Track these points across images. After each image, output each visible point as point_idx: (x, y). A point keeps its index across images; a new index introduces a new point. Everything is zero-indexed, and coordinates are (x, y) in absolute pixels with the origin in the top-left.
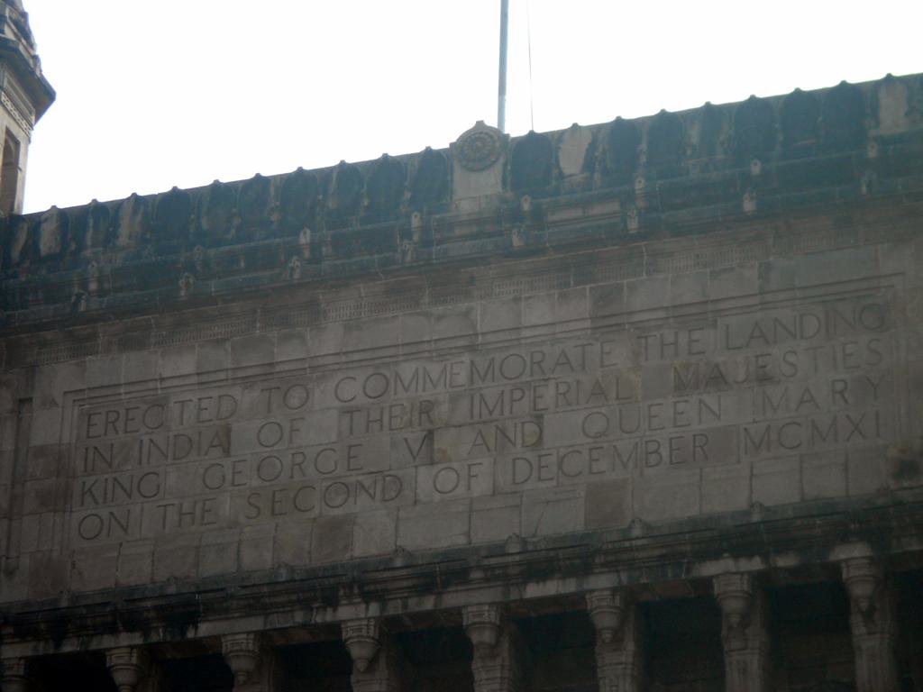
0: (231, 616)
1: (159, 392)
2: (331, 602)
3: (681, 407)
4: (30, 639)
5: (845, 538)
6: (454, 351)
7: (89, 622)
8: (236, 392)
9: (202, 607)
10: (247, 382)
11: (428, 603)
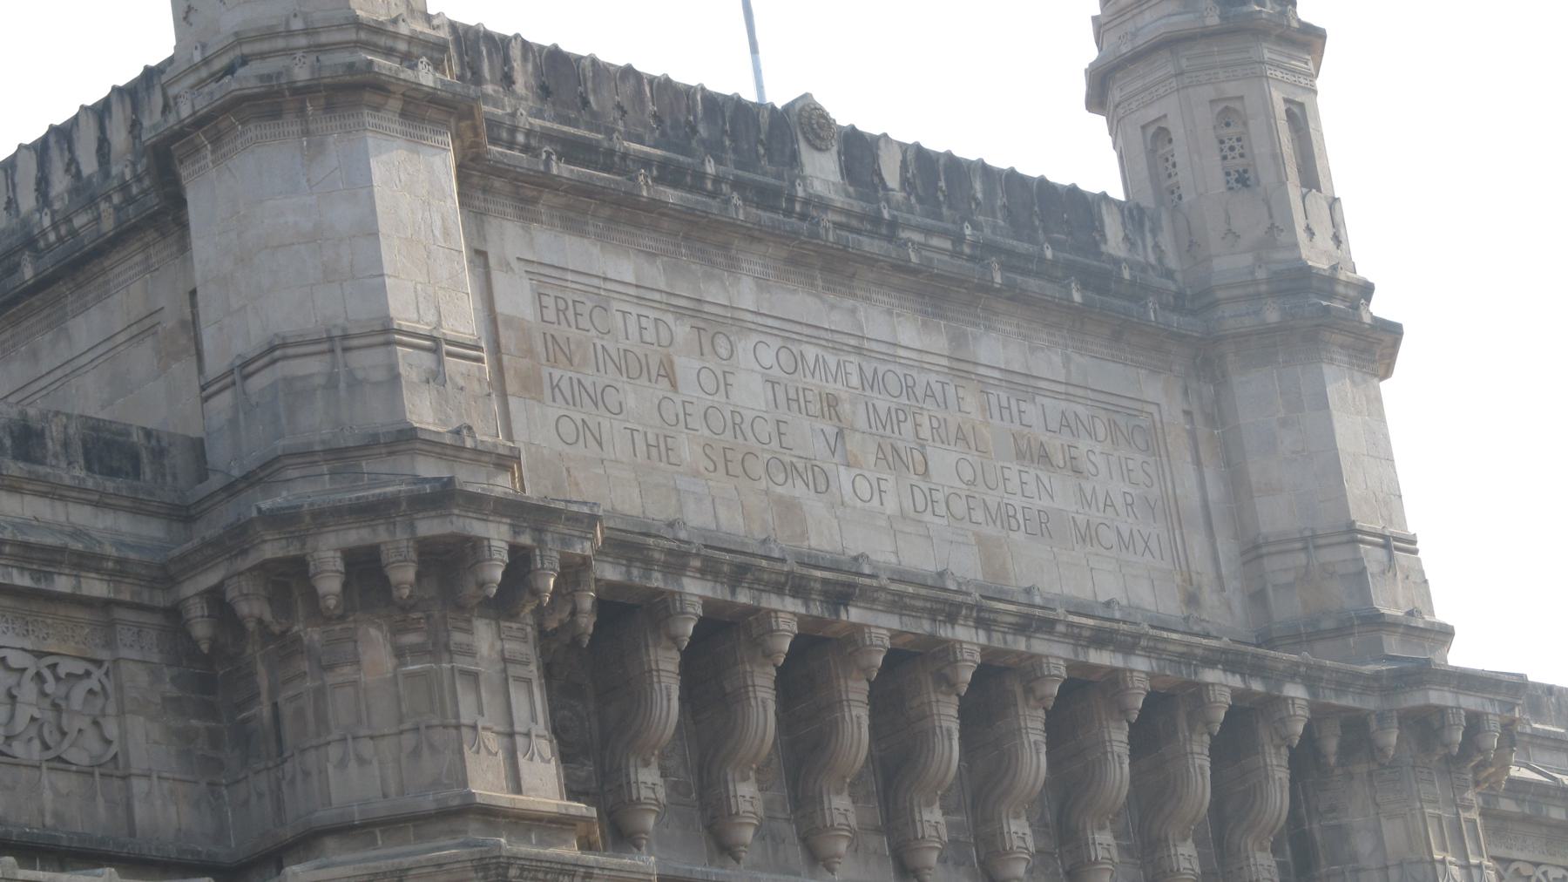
0: (875, 607)
1: (602, 293)
2: (952, 619)
3: (1025, 477)
4: (709, 577)
5: (1293, 674)
6: (845, 348)
7: (766, 576)
8: (669, 318)
9: (857, 591)
10: (680, 312)
11: (1021, 644)
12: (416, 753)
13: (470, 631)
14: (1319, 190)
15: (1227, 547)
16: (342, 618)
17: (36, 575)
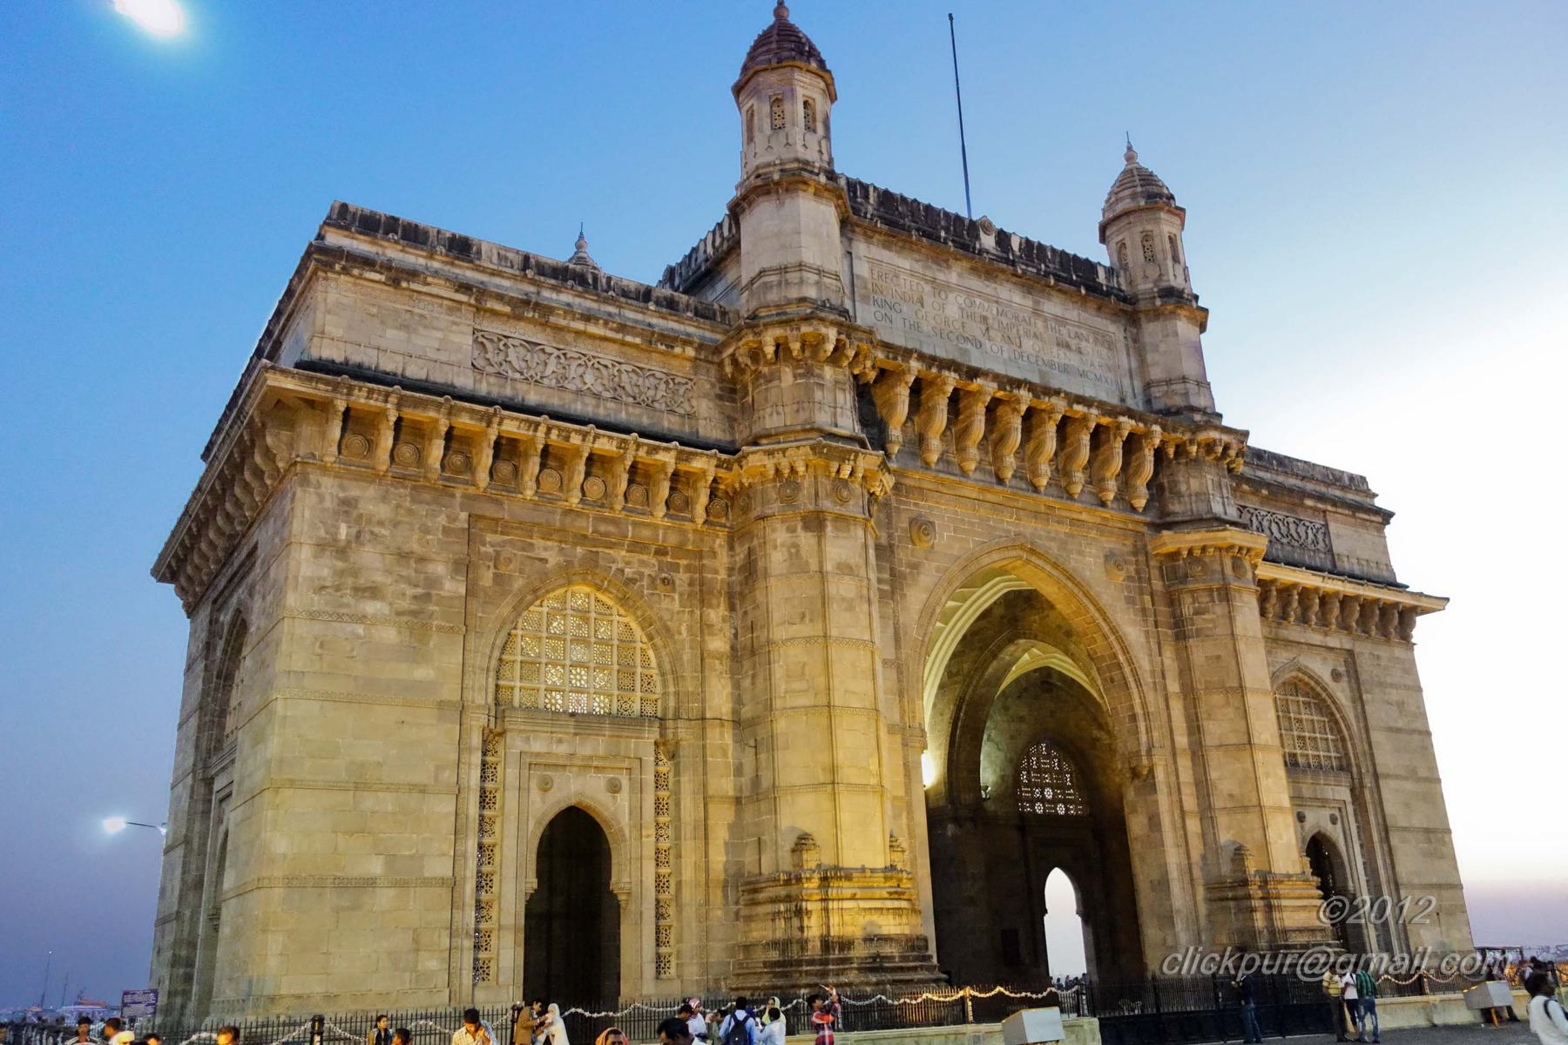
8: (922, 283)
12: (798, 411)
13: (822, 368)
14: (1179, 263)
15: (1138, 384)
16: (775, 364)
17: (667, 346)
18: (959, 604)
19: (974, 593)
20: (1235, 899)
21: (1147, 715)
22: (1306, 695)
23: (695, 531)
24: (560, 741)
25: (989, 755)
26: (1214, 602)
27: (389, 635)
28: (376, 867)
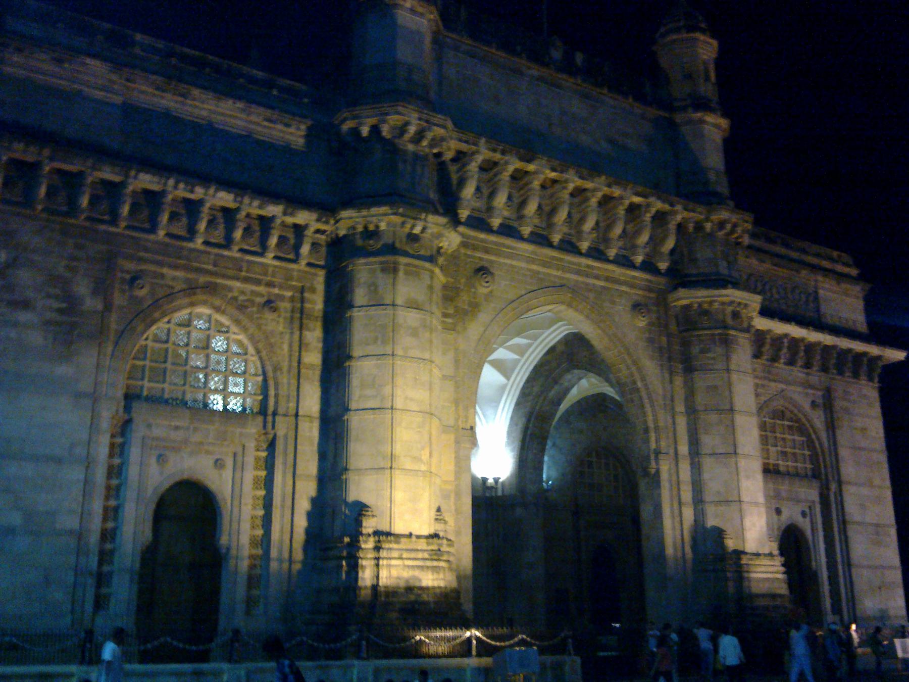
18: (532, 342)
19: (543, 333)
20: (714, 571)
21: (657, 428)
22: (791, 420)
23: (299, 271)
24: (177, 428)
25: (552, 457)
26: (715, 343)
27: (36, 338)
28: (16, 519)
